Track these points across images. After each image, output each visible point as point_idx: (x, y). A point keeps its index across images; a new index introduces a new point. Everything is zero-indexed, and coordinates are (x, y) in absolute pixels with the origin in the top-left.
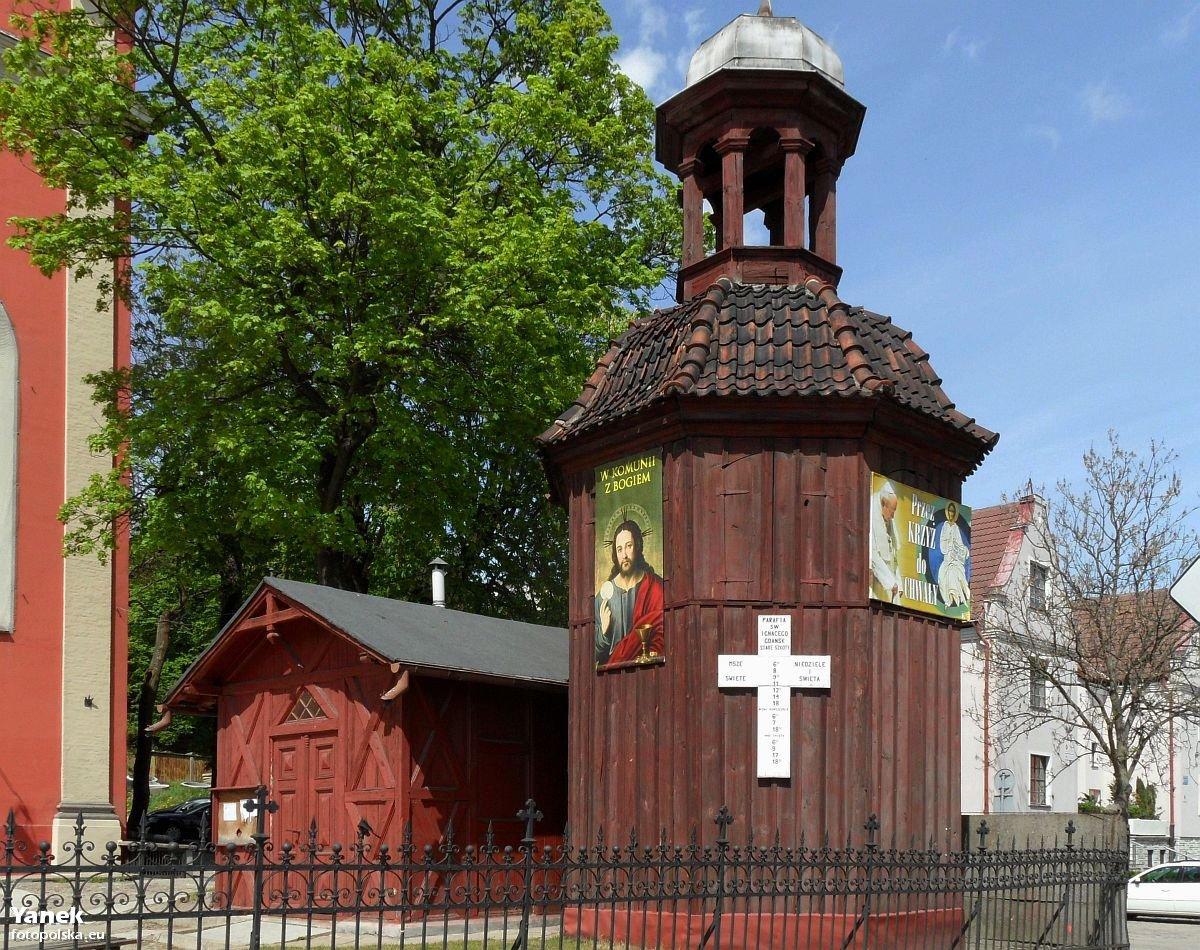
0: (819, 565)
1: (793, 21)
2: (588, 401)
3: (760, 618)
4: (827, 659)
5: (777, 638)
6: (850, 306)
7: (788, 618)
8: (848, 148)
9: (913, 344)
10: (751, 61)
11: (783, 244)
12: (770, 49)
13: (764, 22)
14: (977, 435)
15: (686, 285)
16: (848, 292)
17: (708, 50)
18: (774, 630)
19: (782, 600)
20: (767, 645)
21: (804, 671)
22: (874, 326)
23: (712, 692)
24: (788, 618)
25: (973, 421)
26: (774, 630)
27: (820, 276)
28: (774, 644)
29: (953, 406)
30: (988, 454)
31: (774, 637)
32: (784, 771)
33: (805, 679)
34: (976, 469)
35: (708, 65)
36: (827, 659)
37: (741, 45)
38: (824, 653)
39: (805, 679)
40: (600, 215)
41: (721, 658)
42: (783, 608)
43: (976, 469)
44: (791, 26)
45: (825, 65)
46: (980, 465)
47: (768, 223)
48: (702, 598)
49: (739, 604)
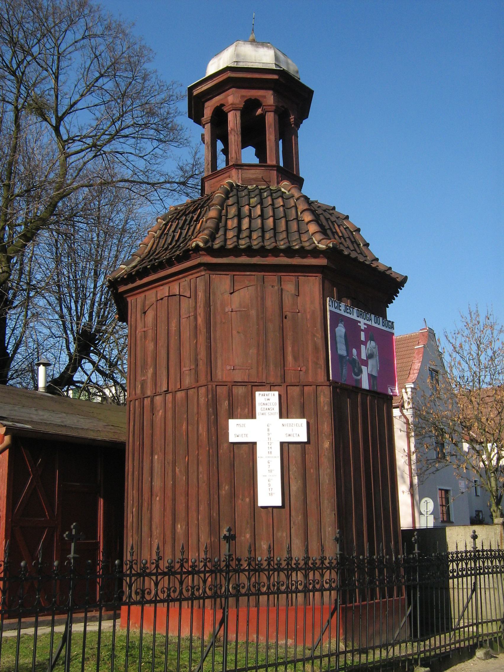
0: (296, 358)
1: (269, 45)
2: (143, 254)
3: (257, 393)
4: (304, 421)
5: (269, 407)
6: (309, 199)
7: (276, 393)
8: (304, 114)
9: (350, 223)
10: (244, 64)
11: (267, 162)
12: (255, 57)
13: (251, 44)
14: (393, 275)
15: (206, 184)
16: (306, 190)
17: (219, 58)
18: (267, 402)
19: (272, 380)
20: (263, 412)
21: (288, 430)
22: (325, 211)
23: (225, 445)
24: (276, 393)
25: (390, 268)
26: (267, 402)
27: (290, 181)
28: (268, 411)
29: (377, 260)
30: (401, 289)
31: (267, 407)
32: (450, 580)
33: (290, 435)
34: (394, 299)
35: (219, 66)
36: (304, 421)
37: (238, 55)
38: (303, 417)
39: (290, 435)
40: (154, 149)
41: (230, 421)
42: (271, 387)
43: (394, 299)
44: (268, 47)
45: (288, 68)
46: (397, 296)
47: (257, 155)
48: (217, 380)
49: (243, 383)
